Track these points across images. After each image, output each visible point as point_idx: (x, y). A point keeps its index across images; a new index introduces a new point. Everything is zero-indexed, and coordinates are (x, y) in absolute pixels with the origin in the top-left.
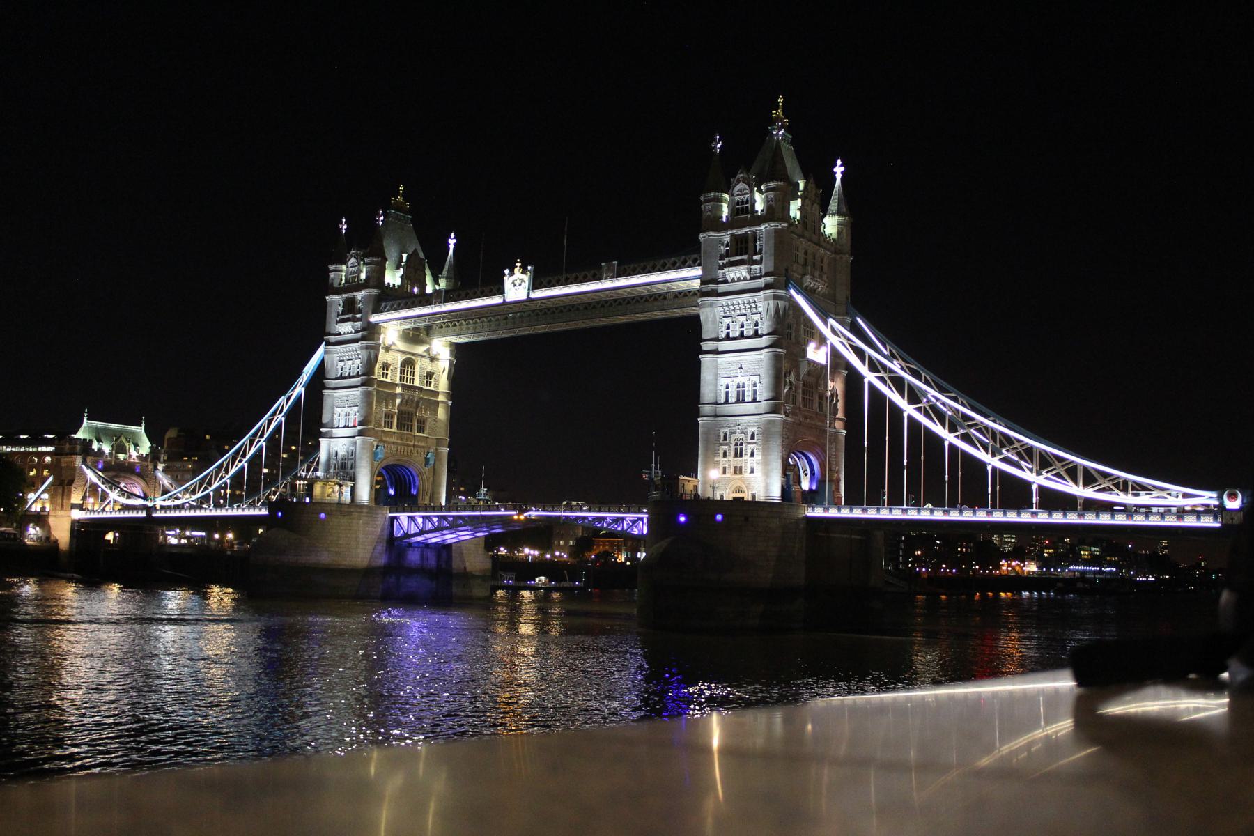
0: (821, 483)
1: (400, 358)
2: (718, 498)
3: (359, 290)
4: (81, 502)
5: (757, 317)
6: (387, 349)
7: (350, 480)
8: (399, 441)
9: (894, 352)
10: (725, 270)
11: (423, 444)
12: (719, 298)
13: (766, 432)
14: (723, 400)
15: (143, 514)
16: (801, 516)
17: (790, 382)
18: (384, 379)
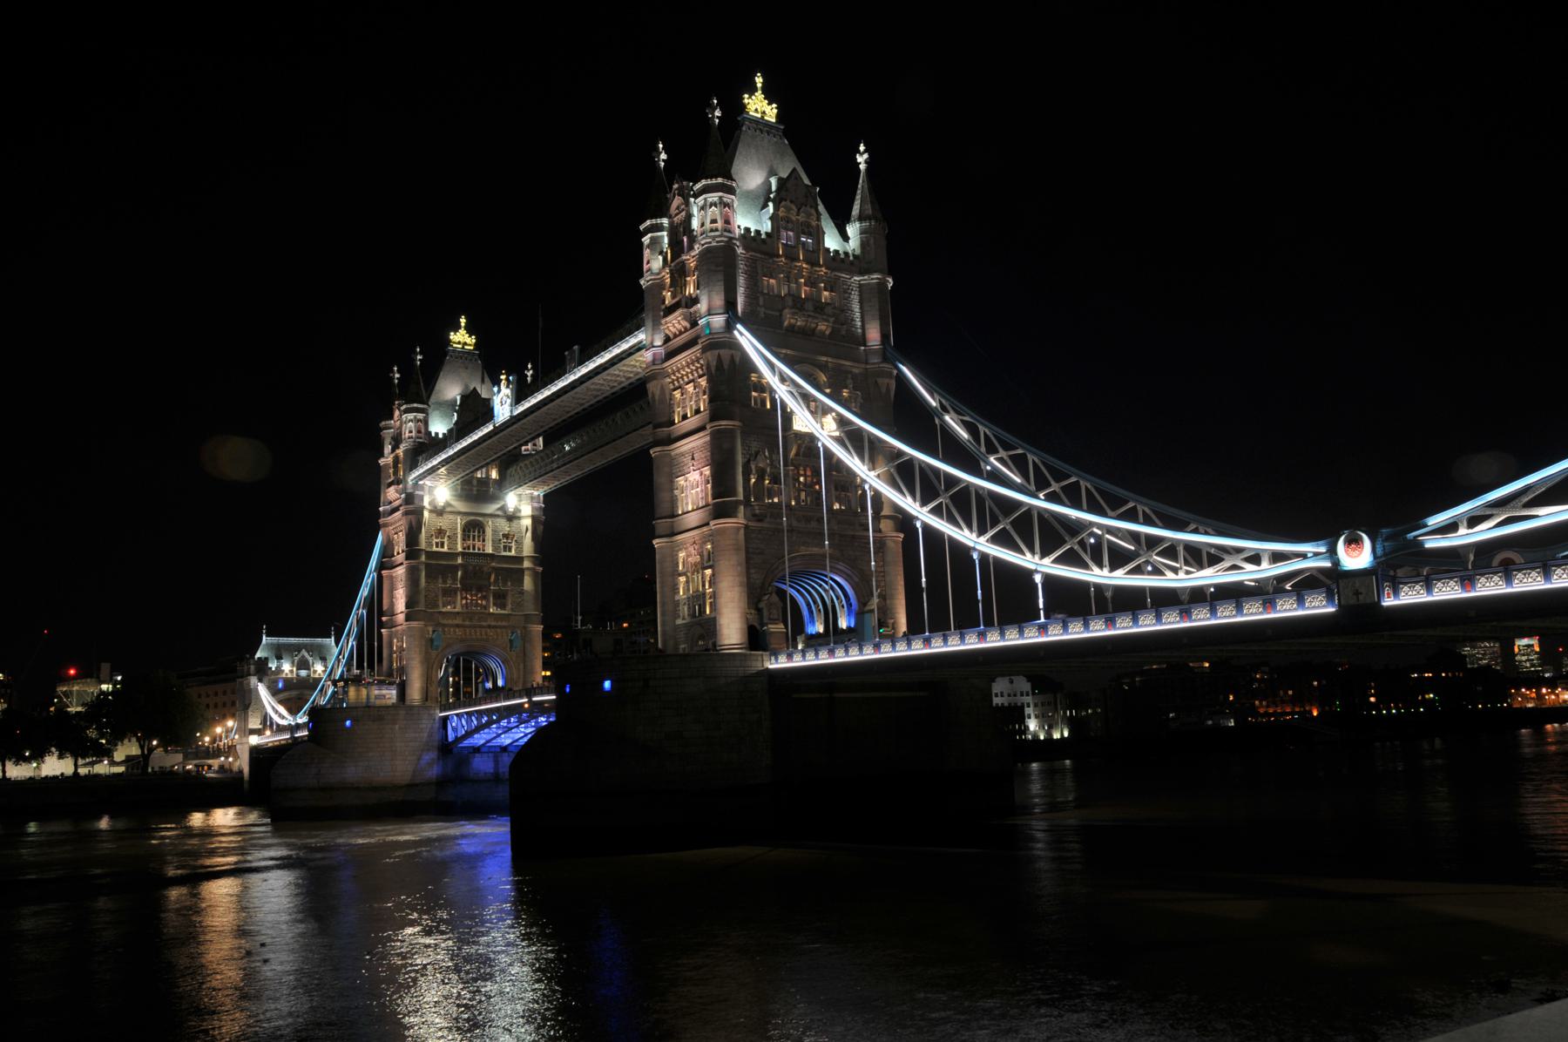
0: (860, 615)
1: (460, 522)
2: (681, 651)
3: (398, 448)
4: (260, 727)
6: (439, 512)
8: (467, 623)
9: (944, 401)
11: (504, 624)
14: (680, 512)
18: (440, 549)
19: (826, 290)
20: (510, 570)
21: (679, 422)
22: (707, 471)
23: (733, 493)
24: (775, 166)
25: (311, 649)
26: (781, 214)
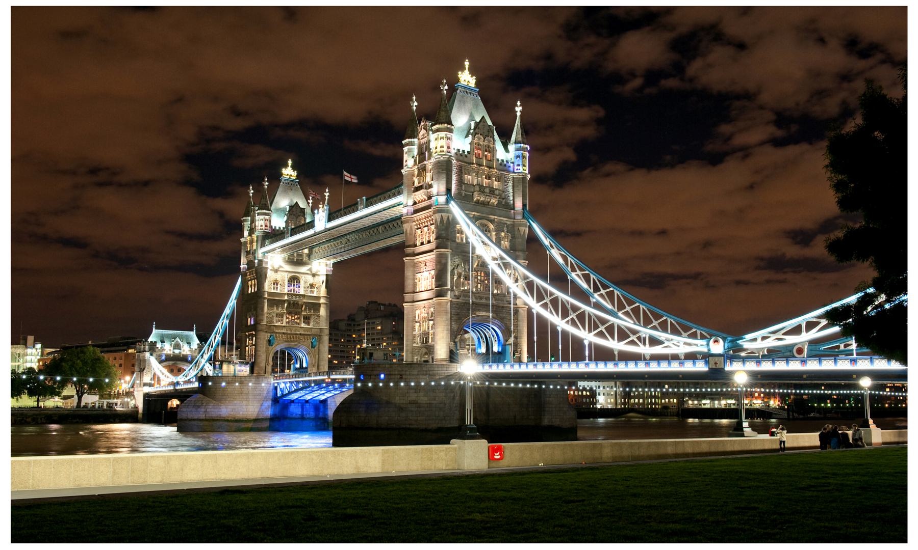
1: (287, 276)
8: (289, 332)
15: (172, 388)
18: (275, 291)
19: (496, 181)
21: (419, 246)
22: (433, 272)
23: (445, 285)
24: (473, 112)
25: (181, 338)
26: (475, 141)
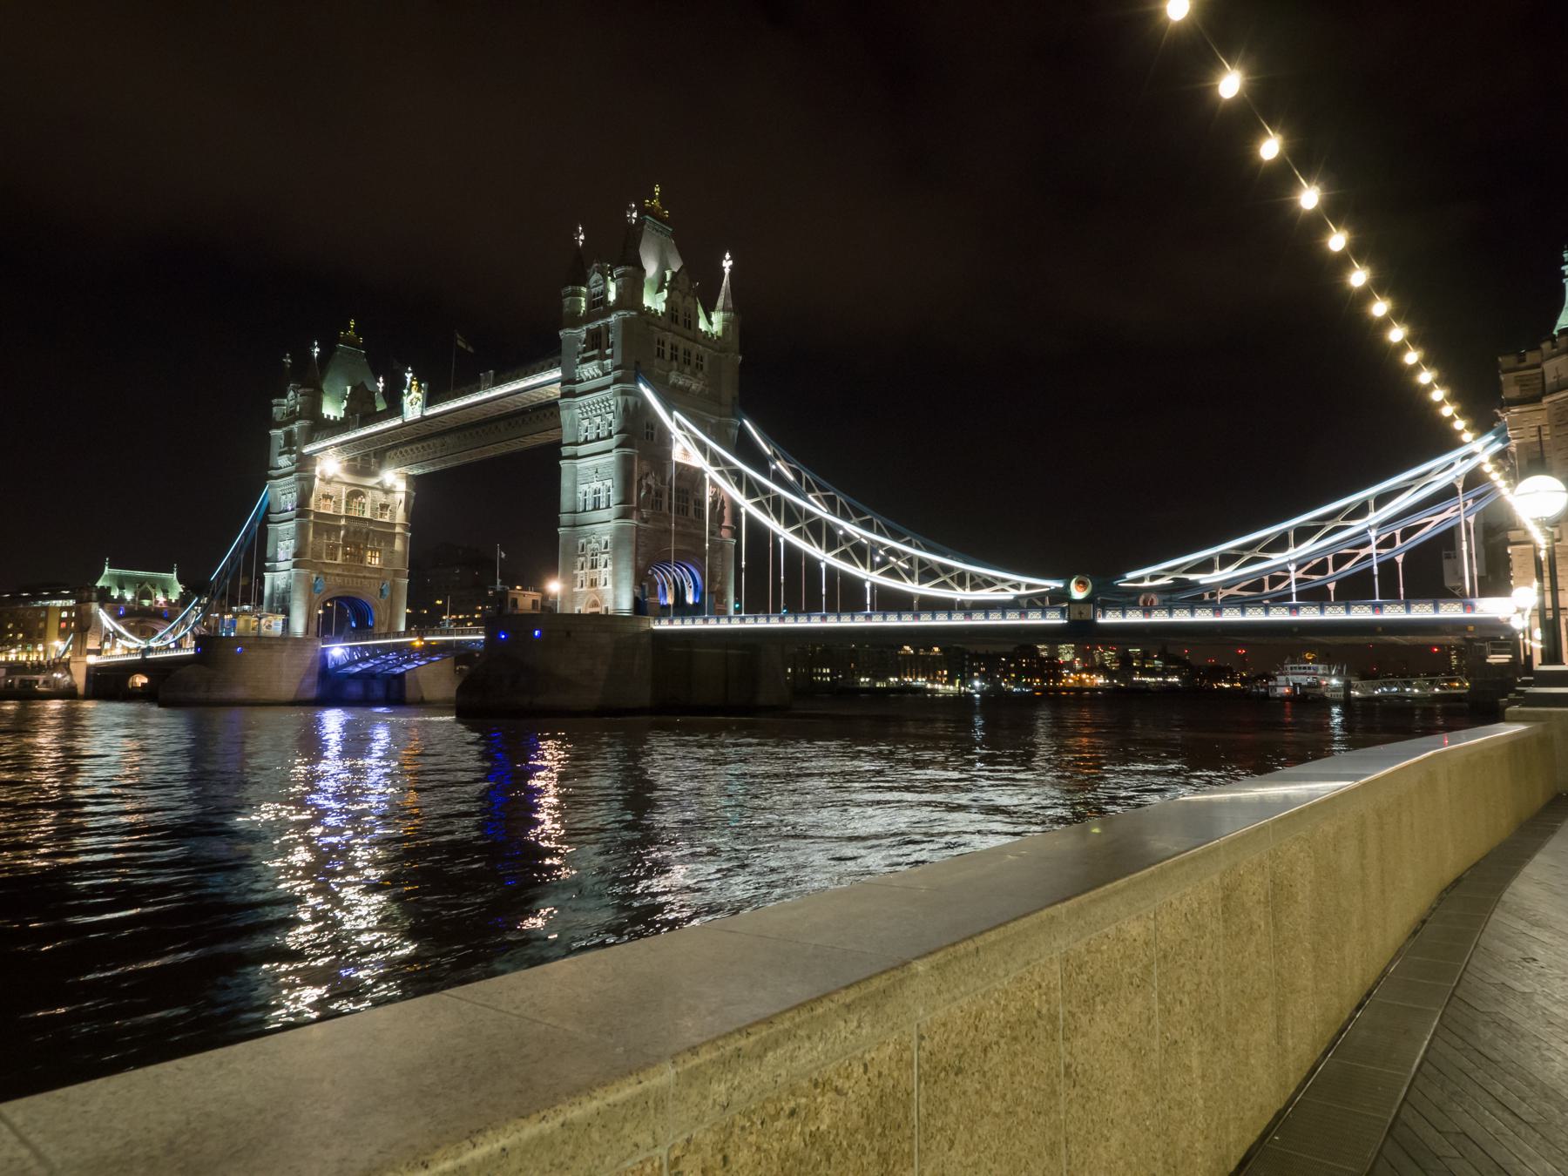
1: (344, 490)
2: (576, 612)
3: (293, 423)
5: (610, 417)
6: (328, 481)
7: (282, 613)
8: (346, 573)
10: (580, 367)
11: (376, 576)
12: (577, 399)
13: (618, 542)
15: (139, 657)
16: (642, 629)
17: (649, 488)
20: (384, 534)
